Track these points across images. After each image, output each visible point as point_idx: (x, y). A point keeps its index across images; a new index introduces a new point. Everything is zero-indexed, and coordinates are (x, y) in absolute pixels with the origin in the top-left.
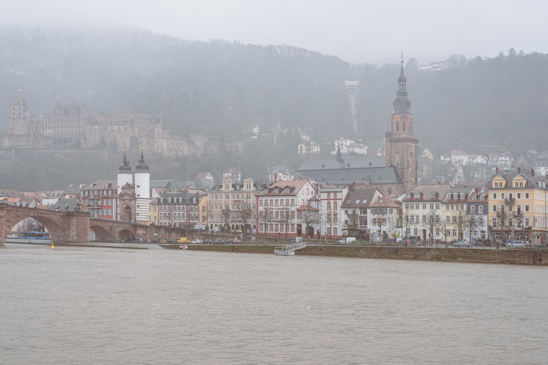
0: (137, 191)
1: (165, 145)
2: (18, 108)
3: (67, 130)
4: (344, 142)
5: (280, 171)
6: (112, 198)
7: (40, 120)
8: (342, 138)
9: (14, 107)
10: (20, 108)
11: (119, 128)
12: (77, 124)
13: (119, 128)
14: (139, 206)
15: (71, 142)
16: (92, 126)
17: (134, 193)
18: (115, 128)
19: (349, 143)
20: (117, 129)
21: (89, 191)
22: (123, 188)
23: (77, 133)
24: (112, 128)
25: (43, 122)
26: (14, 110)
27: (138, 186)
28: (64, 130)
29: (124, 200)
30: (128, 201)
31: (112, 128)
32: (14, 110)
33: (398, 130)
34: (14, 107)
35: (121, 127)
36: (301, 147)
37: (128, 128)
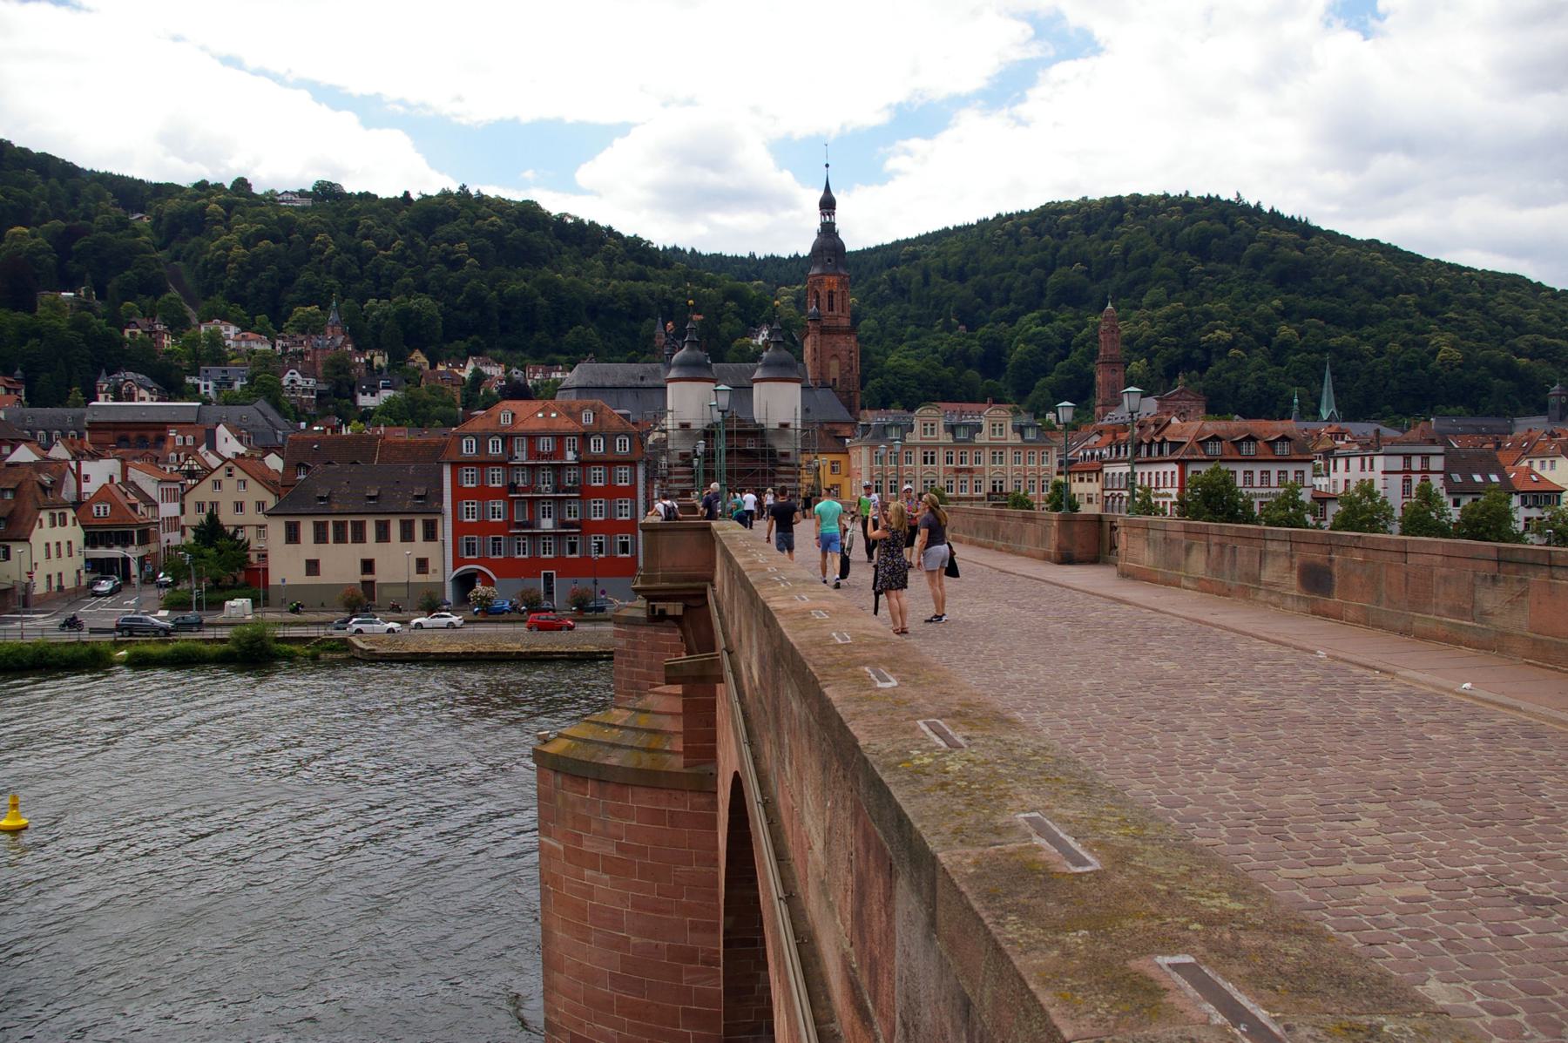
5: (140, 386)
6: (633, 464)
21: (508, 439)
33: (831, 308)
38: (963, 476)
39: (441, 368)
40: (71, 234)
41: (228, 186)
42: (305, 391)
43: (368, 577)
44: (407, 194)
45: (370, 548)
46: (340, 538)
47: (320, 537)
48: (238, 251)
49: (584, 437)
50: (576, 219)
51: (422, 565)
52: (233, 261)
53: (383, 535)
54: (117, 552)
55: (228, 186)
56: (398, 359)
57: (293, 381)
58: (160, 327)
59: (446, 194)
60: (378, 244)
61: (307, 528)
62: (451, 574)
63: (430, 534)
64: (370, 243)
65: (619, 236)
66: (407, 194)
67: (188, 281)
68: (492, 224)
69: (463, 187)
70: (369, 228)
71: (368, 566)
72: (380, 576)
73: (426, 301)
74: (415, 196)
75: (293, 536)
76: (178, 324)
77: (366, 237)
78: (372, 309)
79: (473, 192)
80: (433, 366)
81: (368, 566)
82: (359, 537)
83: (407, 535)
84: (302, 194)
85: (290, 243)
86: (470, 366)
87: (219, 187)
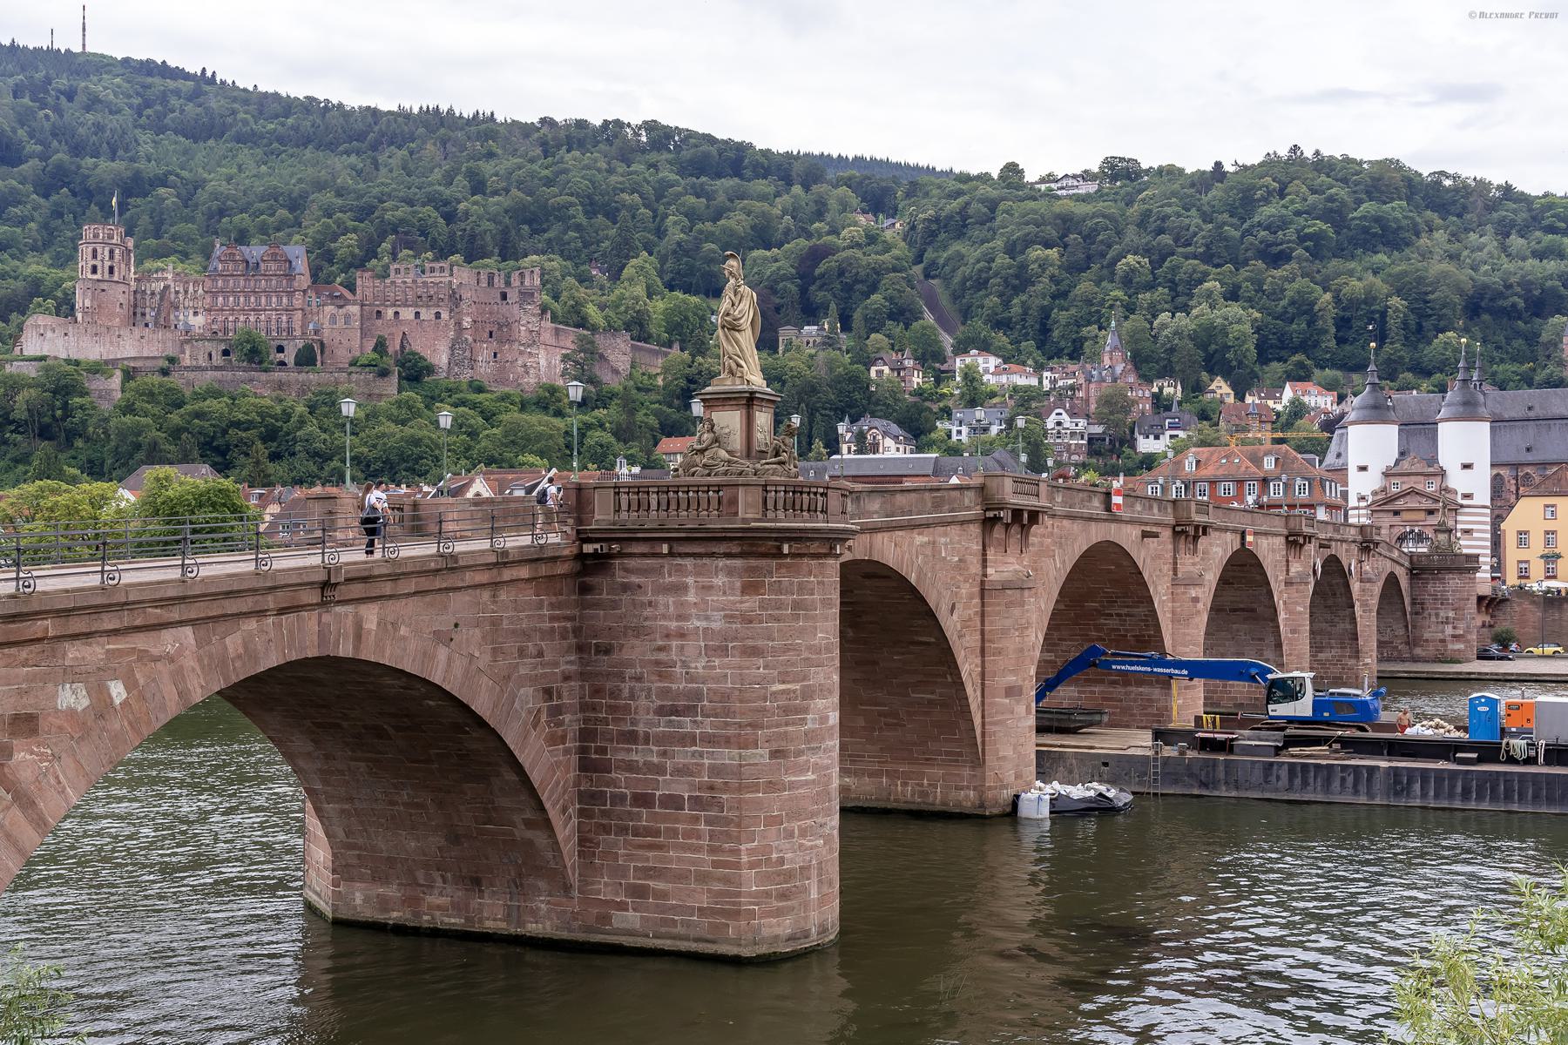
1: (543, 362)
2: (107, 253)
3: (252, 319)
4: (980, 360)
5: (885, 434)
7: (167, 287)
8: (974, 352)
9: (95, 251)
10: (112, 252)
11: (417, 314)
12: (285, 300)
13: (417, 314)
14: (1467, 532)
15: (280, 349)
16: (341, 307)
18: (407, 314)
19: (993, 362)
20: (412, 316)
22: (1387, 474)
23: (284, 325)
24: (397, 313)
25: (177, 292)
26: (95, 256)
27: (1467, 466)
28: (242, 318)
29: (1396, 513)
30: (1422, 515)
31: (397, 313)
32: (95, 256)
34: (95, 251)
35: (423, 311)
36: (880, 373)
37: (445, 315)
39: (1249, 399)
40: (817, 255)
41: (995, 176)
42: (1073, 434)
44: (1218, 165)
48: (1002, 260)
49: (1265, 482)
50: (1455, 177)
52: (996, 275)
55: (995, 176)
56: (1195, 389)
57: (1059, 424)
58: (909, 363)
59: (1271, 163)
60: (1176, 240)
64: (1166, 239)
65: (1523, 198)
66: (1218, 165)
67: (944, 300)
68: (1331, 199)
69: (1295, 148)
70: (1165, 218)
73: (1235, 309)
74: (1229, 168)
76: (930, 357)
77: (1160, 231)
78: (1164, 326)
79: (1308, 153)
80: (1240, 397)
84: (1086, 176)
85: (1066, 246)
86: (1288, 393)
87: (984, 178)
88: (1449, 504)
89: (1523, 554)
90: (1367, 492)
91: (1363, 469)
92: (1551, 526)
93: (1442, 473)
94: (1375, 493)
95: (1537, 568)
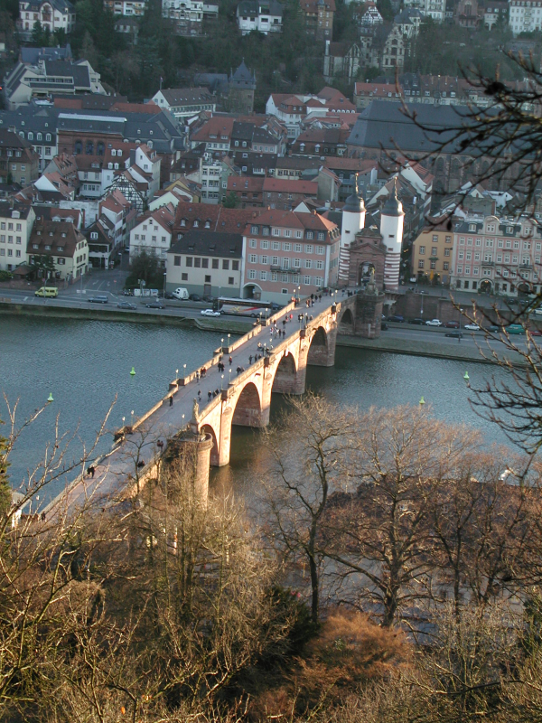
0: (387, 242)
17: (383, 247)
27: (391, 236)
38: (508, 253)
43: (207, 283)
45: (209, 271)
46: (197, 265)
47: (189, 264)
51: (231, 280)
53: (215, 265)
54: (99, 255)
61: (184, 258)
62: (243, 285)
63: (236, 267)
71: (208, 278)
72: (213, 283)
75: (177, 262)
81: (208, 278)
82: (205, 265)
83: (226, 266)
88: (382, 250)
89: (422, 257)
90: (348, 243)
91: (347, 232)
92: (435, 245)
93: (382, 238)
94: (352, 244)
95: (427, 265)
